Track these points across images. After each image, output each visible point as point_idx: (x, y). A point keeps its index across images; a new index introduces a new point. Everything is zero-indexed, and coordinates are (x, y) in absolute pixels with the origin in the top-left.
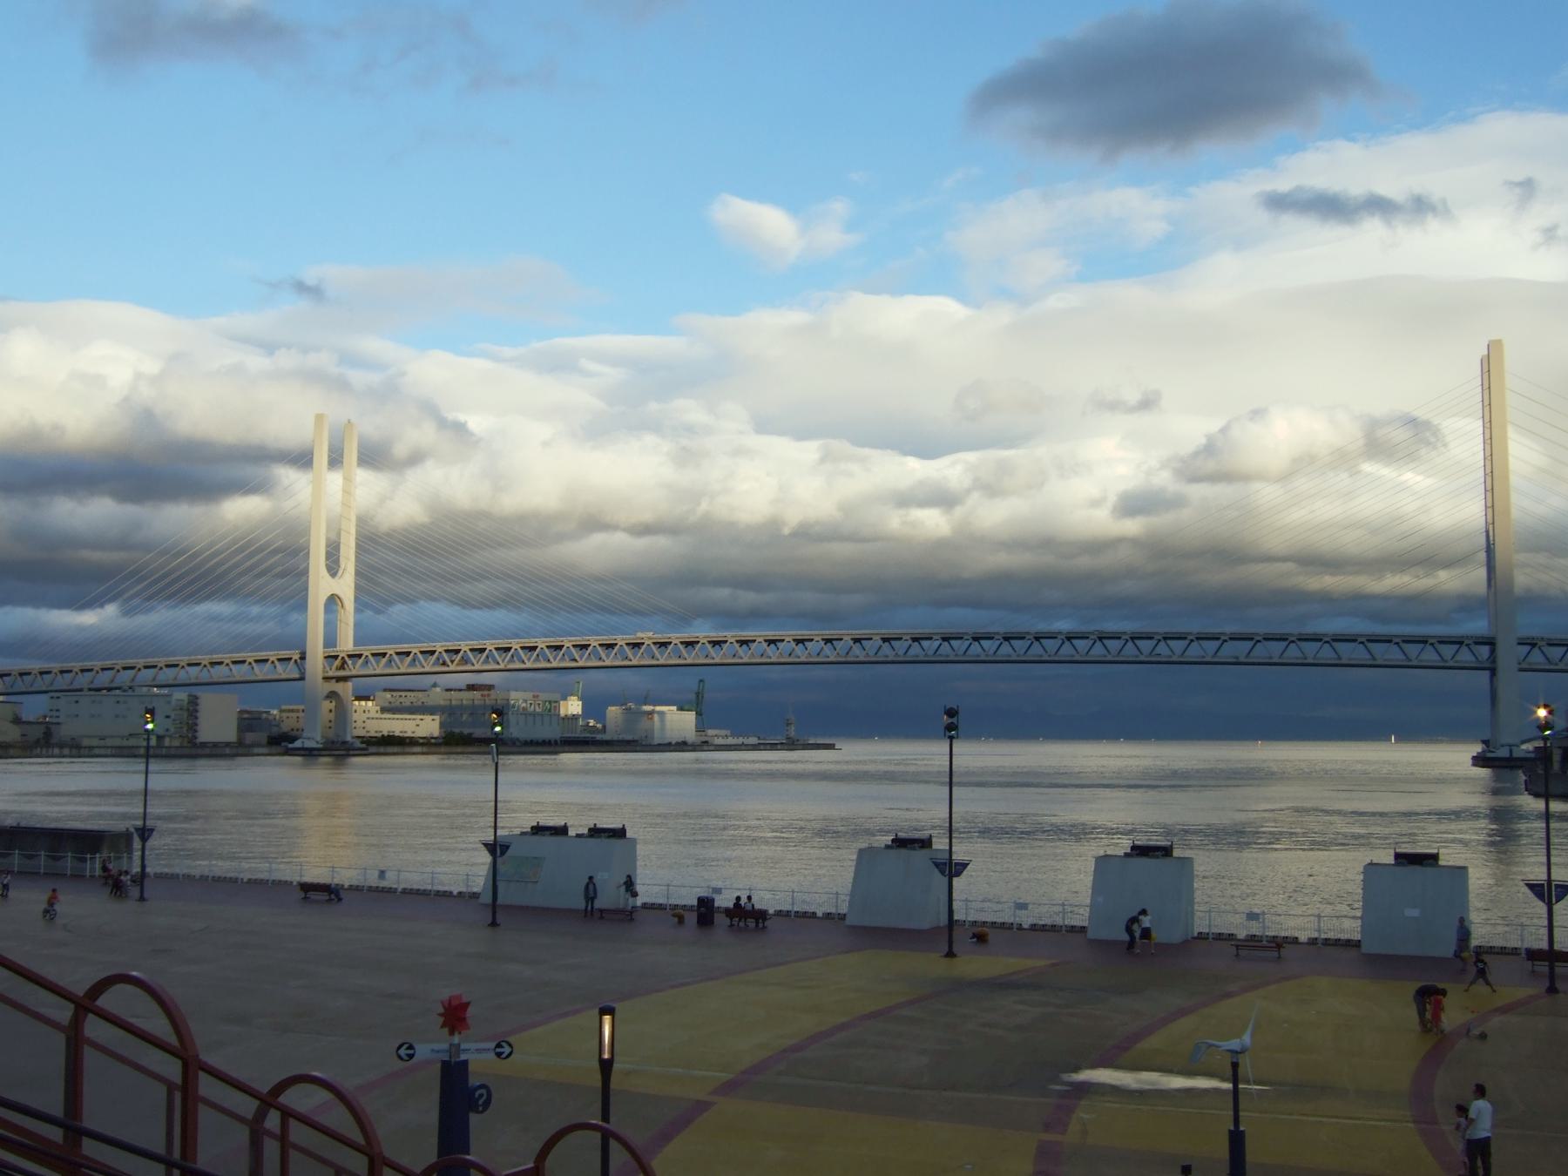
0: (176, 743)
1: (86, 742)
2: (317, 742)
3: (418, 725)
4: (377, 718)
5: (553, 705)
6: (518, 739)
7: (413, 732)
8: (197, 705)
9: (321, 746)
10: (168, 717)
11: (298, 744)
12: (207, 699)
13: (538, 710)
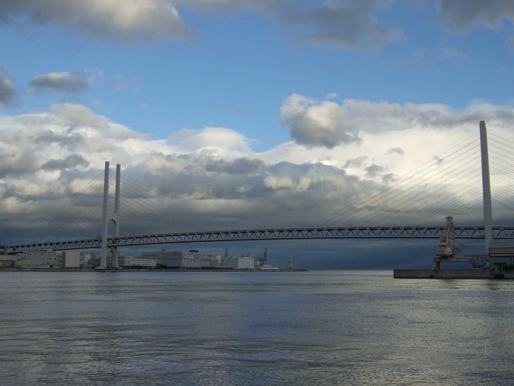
0: (58, 267)
1: (23, 267)
2: (105, 267)
3: (148, 262)
4: (133, 260)
5: (198, 256)
6: (185, 267)
7: (147, 265)
8: (65, 255)
9: (105, 268)
10: (55, 259)
11: (98, 268)
12: (68, 253)
13: (193, 257)
